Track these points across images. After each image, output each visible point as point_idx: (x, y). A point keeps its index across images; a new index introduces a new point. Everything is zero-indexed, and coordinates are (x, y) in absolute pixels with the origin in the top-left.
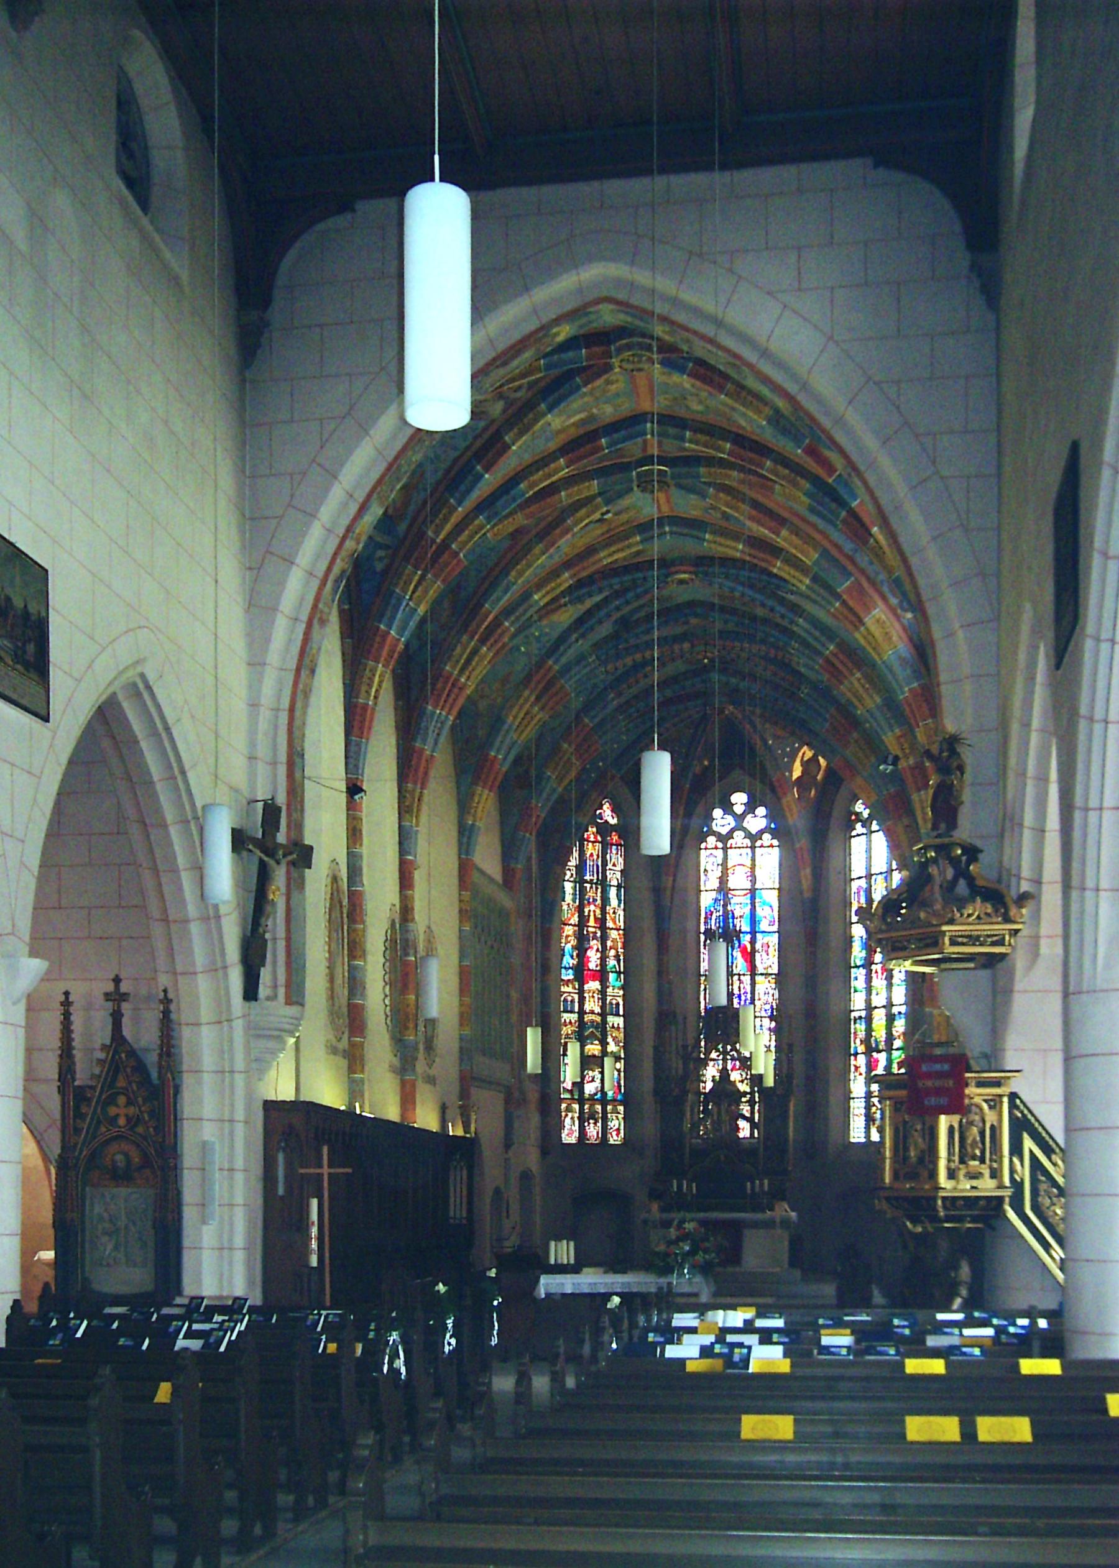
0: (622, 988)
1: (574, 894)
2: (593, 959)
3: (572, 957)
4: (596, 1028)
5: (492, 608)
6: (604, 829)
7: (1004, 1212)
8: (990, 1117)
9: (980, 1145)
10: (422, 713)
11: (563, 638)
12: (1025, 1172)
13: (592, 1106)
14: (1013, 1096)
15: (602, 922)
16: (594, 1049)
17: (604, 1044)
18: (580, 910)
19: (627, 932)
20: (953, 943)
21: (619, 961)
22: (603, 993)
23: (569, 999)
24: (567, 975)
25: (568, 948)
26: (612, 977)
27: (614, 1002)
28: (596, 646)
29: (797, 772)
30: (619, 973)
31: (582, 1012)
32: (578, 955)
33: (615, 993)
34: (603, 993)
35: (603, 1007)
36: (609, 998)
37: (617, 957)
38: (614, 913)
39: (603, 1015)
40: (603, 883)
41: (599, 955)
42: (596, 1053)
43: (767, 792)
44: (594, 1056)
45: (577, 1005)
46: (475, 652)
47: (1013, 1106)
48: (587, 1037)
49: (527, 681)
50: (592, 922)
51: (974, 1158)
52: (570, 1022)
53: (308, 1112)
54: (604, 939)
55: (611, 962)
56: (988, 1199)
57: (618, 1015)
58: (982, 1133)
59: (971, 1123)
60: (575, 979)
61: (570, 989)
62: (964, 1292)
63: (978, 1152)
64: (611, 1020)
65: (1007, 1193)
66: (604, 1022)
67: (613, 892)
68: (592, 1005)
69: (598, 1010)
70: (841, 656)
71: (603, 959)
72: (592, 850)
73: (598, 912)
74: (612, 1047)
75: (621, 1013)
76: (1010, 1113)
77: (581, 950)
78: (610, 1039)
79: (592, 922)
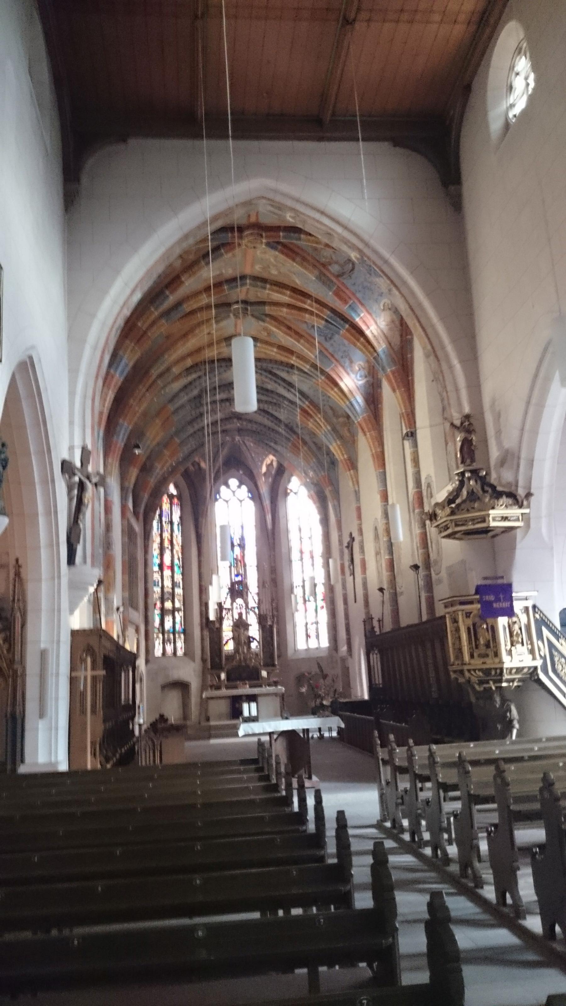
1: (158, 529)
5: (155, 372)
6: (171, 497)
7: (537, 675)
8: (523, 619)
9: (521, 636)
10: (117, 424)
11: (176, 396)
12: (545, 651)
14: (534, 607)
18: (161, 536)
20: (494, 520)
22: (173, 577)
24: (156, 568)
26: (176, 569)
28: (190, 401)
29: (264, 469)
30: (179, 567)
33: (178, 577)
34: (173, 577)
39: (173, 589)
40: (171, 523)
43: (250, 478)
46: (144, 395)
47: (534, 612)
49: (158, 414)
51: (518, 642)
53: (101, 637)
54: (172, 551)
56: (529, 668)
58: (520, 629)
59: (515, 623)
62: (517, 726)
63: (520, 640)
65: (538, 663)
67: (175, 527)
68: (168, 583)
69: (170, 586)
70: (311, 407)
72: (166, 506)
76: (534, 617)
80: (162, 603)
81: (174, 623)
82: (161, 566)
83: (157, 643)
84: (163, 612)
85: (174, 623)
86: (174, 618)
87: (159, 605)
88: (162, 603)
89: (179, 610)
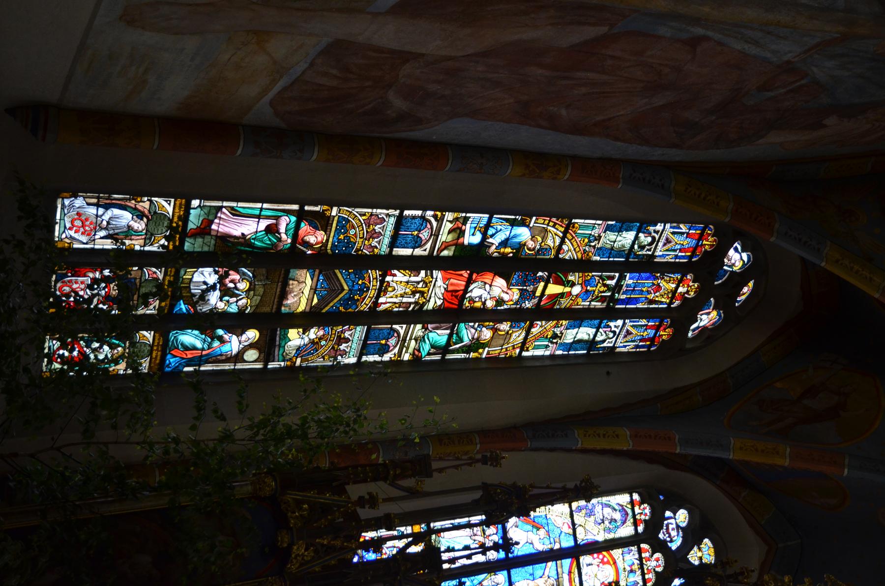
0: (416, 359)
2: (491, 290)
3: (504, 243)
4: (346, 302)
13: (159, 290)
15: (549, 311)
16: (302, 292)
17: (305, 320)
18: (583, 265)
19: (515, 366)
21: (468, 349)
23: (425, 235)
25: (523, 234)
26: (440, 336)
27: (392, 341)
30: (444, 350)
31: (388, 263)
32: (504, 256)
34: (416, 315)
35: (391, 316)
36: (401, 329)
37: (476, 345)
38: (555, 336)
39: (373, 317)
41: (490, 304)
42: (290, 301)
44: (284, 295)
45: (407, 252)
48: (331, 279)
50: (554, 289)
52: (373, 235)
54: (516, 315)
55: (467, 333)
57: (364, 349)
60: (461, 248)
61: (444, 236)
64: (357, 333)
66: (355, 319)
67: (585, 333)
69: (386, 302)
71: (481, 315)
73: (565, 303)
74: (295, 338)
75: (364, 358)
77: (515, 265)
78: (313, 333)
79: (554, 289)
80: (322, 262)
81: (209, 323)
82: (474, 261)
83: (124, 218)
84: (273, 263)
85: (209, 323)
86: (236, 323)
87: (315, 237)
88: (322, 262)
89: (268, 347)
